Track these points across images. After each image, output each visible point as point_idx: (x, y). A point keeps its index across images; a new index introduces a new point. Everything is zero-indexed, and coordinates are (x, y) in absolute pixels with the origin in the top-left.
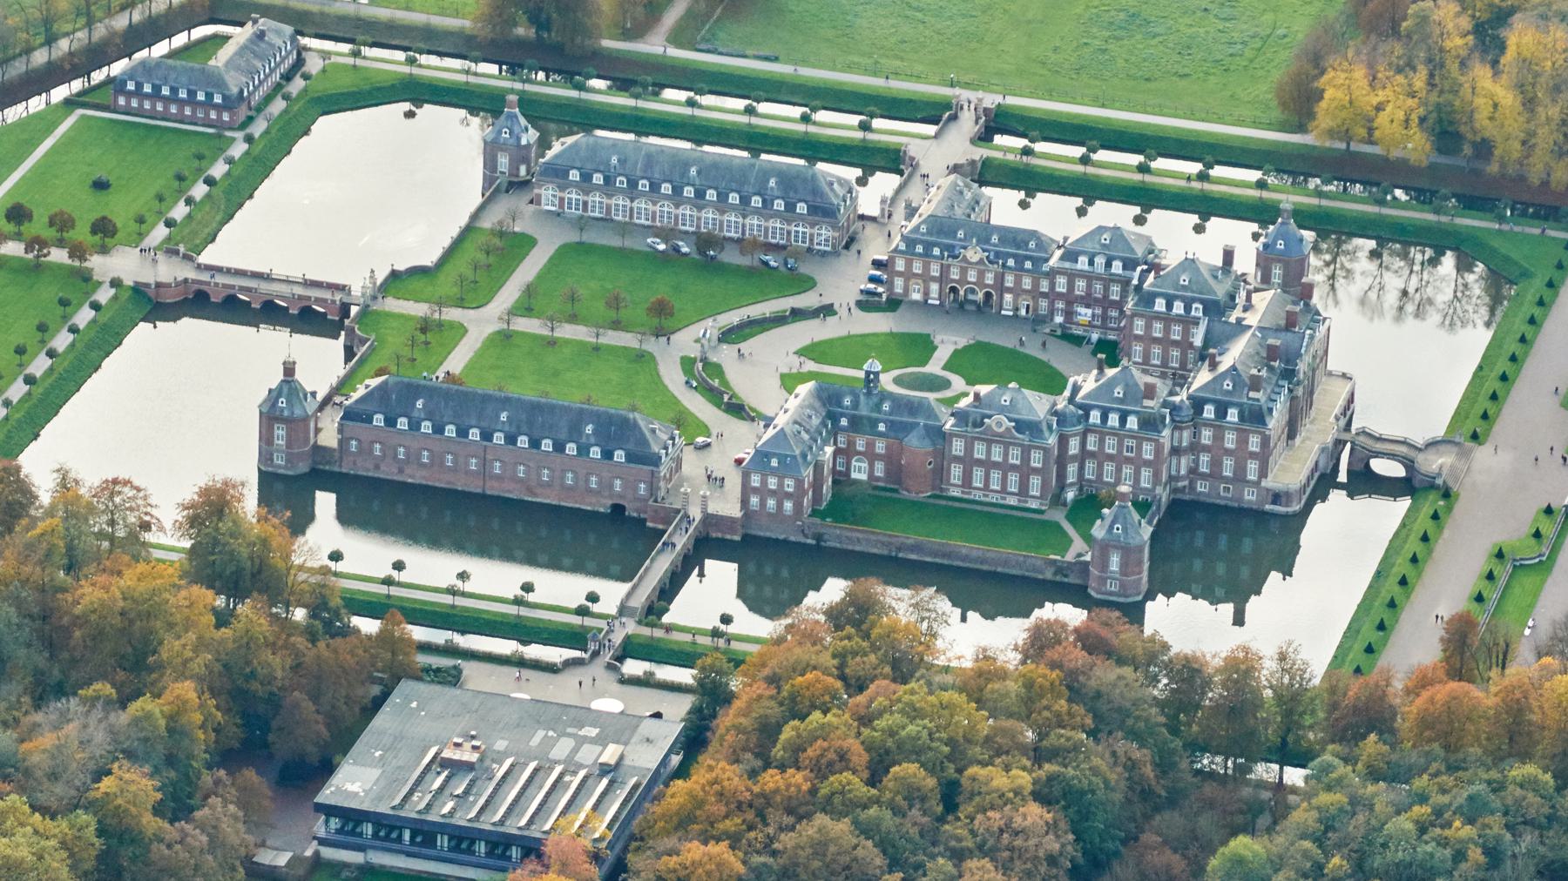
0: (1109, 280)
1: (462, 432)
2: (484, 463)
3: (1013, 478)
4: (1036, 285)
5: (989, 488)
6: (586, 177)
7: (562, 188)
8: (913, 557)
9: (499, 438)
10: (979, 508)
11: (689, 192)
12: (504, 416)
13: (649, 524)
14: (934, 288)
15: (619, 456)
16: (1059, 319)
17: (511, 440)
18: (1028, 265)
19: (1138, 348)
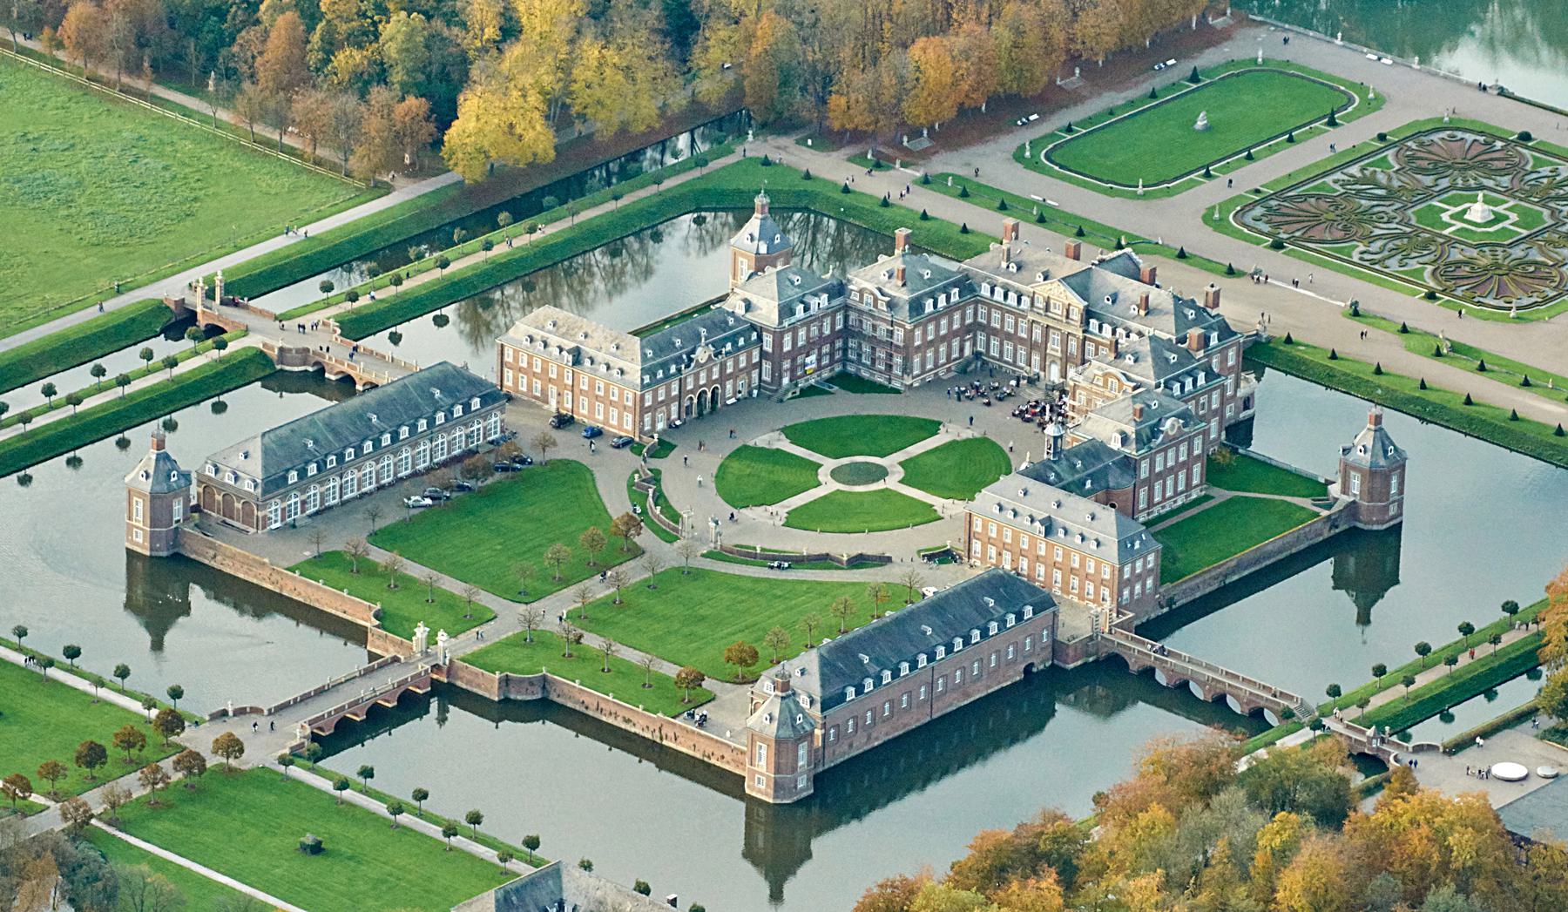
0: (820, 319)
1: (914, 665)
2: (932, 686)
3: (1182, 476)
4: (749, 358)
5: (1169, 495)
6: (302, 474)
7: (284, 498)
8: (1236, 578)
9: (941, 650)
10: (1175, 520)
11: (386, 439)
12: (929, 631)
13: (1071, 666)
14: (674, 408)
15: (1028, 610)
16: (786, 381)
17: (949, 649)
18: (741, 342)
19: (917, 360)
